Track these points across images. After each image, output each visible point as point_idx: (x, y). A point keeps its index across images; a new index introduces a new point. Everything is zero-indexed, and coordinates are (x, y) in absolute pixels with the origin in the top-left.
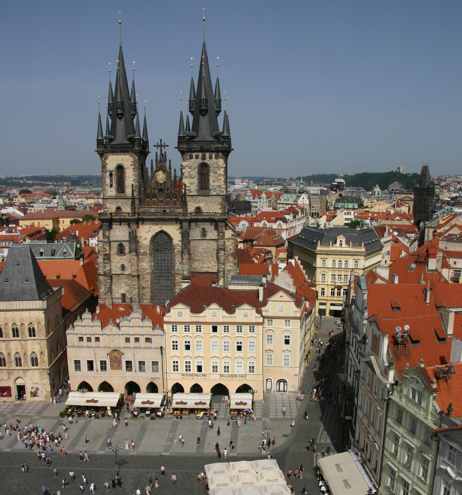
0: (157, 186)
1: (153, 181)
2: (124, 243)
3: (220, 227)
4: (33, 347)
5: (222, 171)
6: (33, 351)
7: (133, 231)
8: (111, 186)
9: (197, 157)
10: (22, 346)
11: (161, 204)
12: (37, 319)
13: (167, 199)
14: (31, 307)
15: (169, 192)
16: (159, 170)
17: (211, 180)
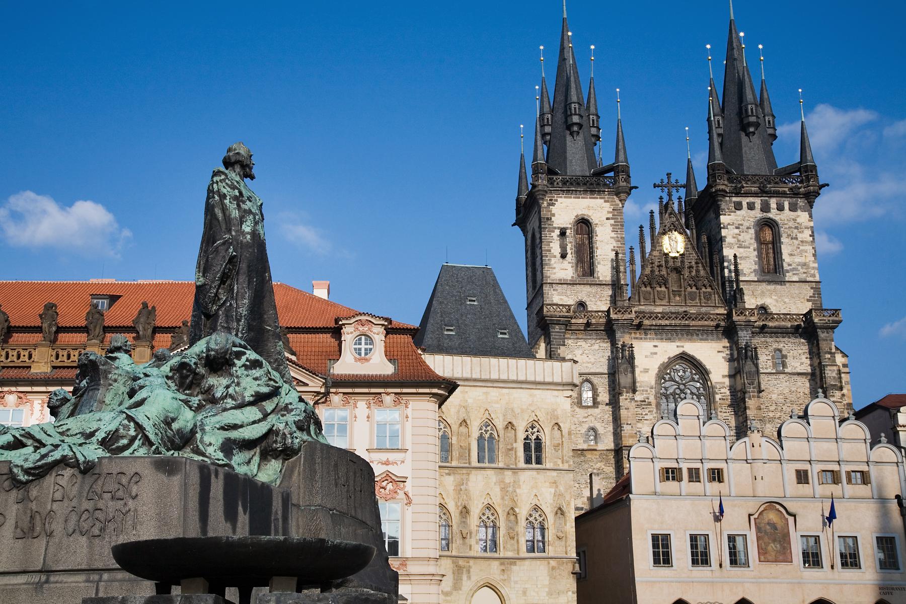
0: (667, 262)
1: (656, 253)
2: (595, 380)
3: (824, 340)
4: (535, 491)
5: (806, 235)
6: (535, 502)
7: (624, 346)
8: (564, 256)
9: (751, 207)
10: (504, 490)
11: (678, 298)
12: (552, 413)
13: (689, 289)
14: (539, 379)
15: (694, 274)
16: (670, 230)
17: (786, 250)
